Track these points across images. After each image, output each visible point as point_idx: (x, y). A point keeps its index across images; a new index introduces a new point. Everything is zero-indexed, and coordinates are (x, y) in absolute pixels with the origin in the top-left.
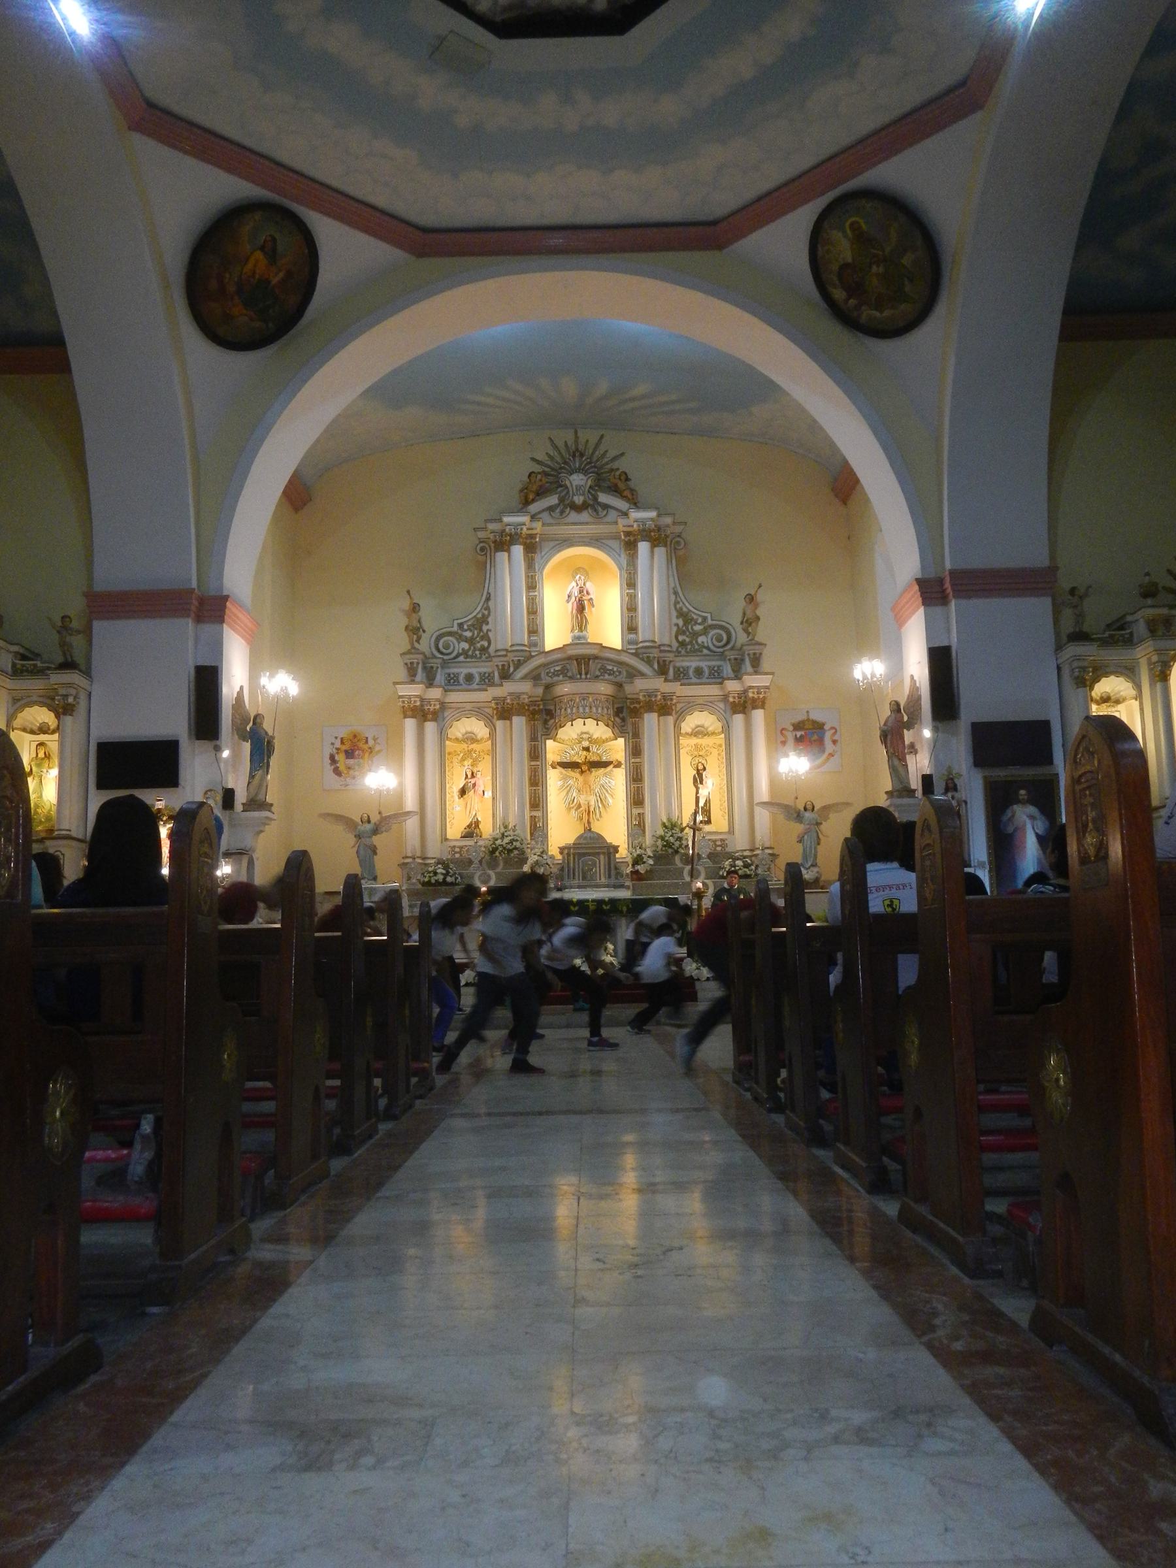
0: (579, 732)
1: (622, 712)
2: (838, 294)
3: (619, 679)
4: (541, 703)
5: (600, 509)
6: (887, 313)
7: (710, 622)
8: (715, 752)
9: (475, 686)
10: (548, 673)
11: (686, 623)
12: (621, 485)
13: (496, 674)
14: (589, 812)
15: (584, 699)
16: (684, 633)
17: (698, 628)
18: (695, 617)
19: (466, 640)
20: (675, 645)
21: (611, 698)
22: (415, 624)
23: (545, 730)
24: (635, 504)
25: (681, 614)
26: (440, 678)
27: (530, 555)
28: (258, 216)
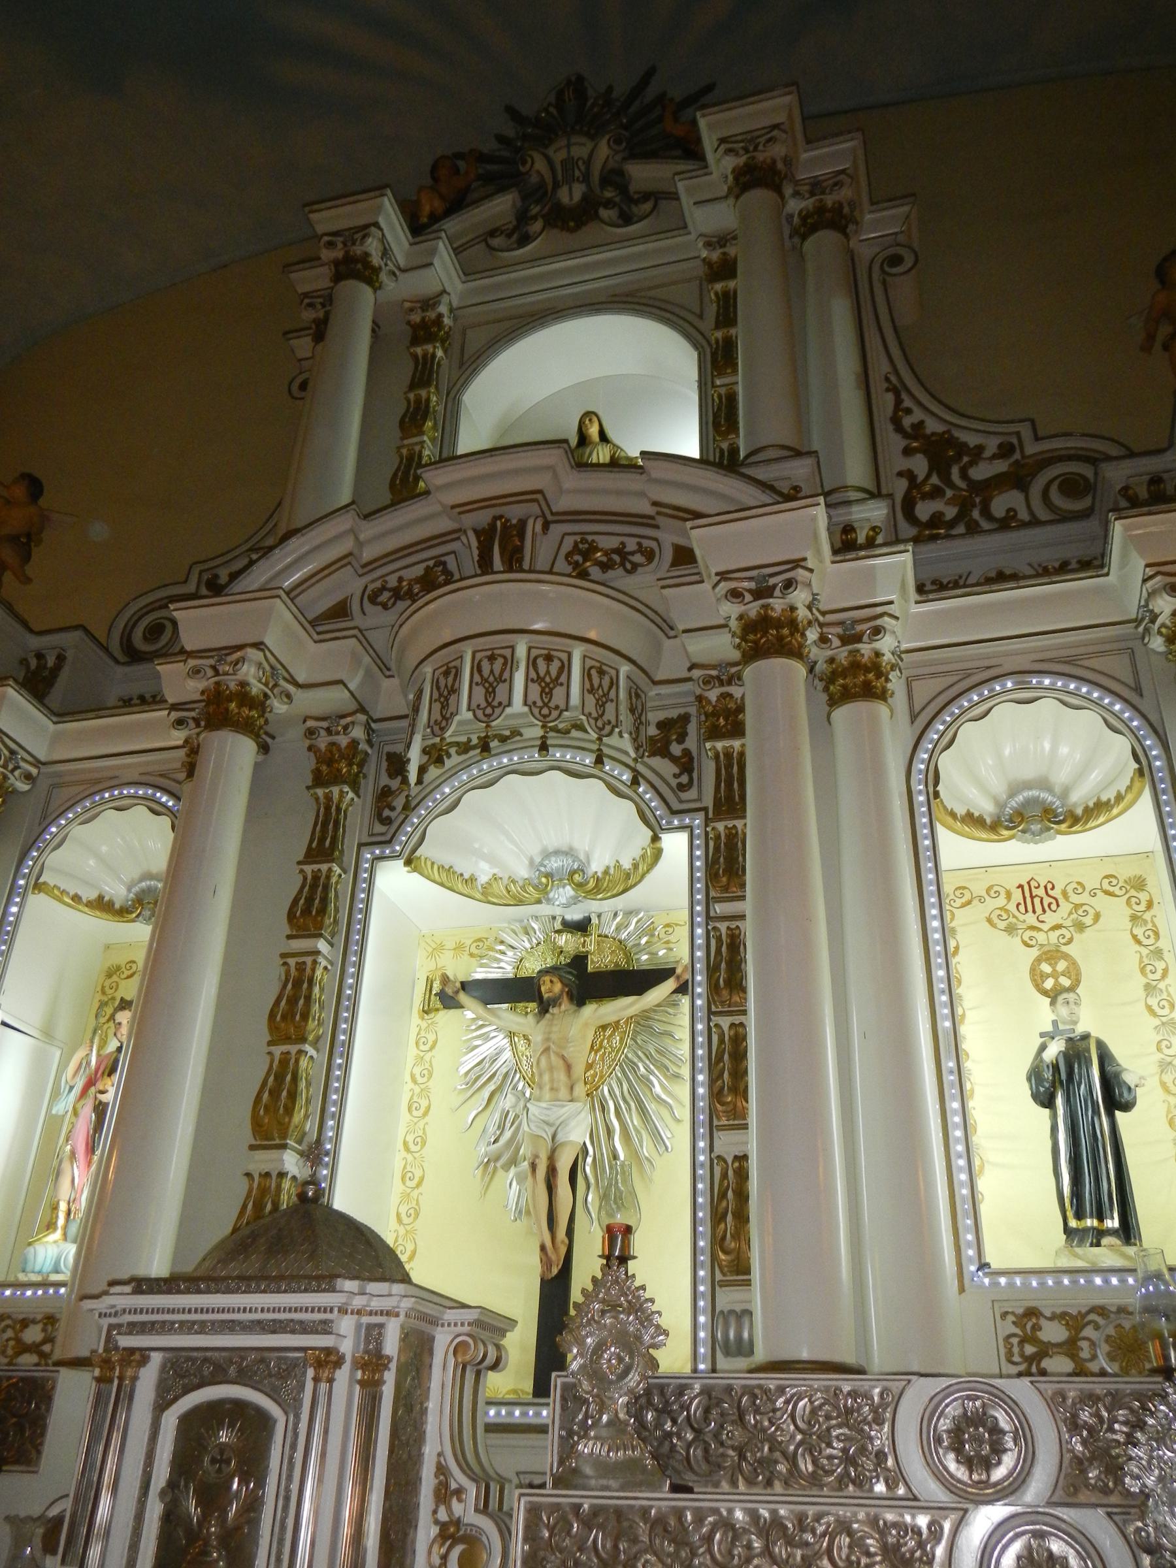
0: (535, 851)
1: (681, 739)
4: (362, 718)
5: (635, 209)
7: (1031, 449)
8: (1115, 912)
10: (373, 599)
11: (939, 465)
14: (552, 1171)
15: (492, 658)
16: (937, 493)
18: (972, 440)
21: (625, 669)
23: (379, 828)
27: (419, 350)
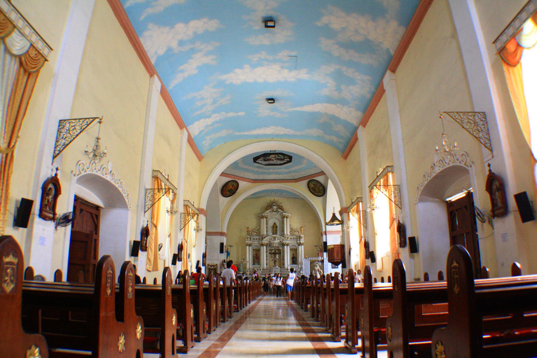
2: (312, 191)
3: (281, 240)
6: (318, 194)
7: (296, 230)
9: (257, 240)
12: (282, 208)
13: (261, 238)
17: (293, 231)
19: (256, 232)
20: (290, 234)
22: (248, 230)
24: (283, 211)
25: (291, 229)
26: (252, 240)
28: (232, 182)
